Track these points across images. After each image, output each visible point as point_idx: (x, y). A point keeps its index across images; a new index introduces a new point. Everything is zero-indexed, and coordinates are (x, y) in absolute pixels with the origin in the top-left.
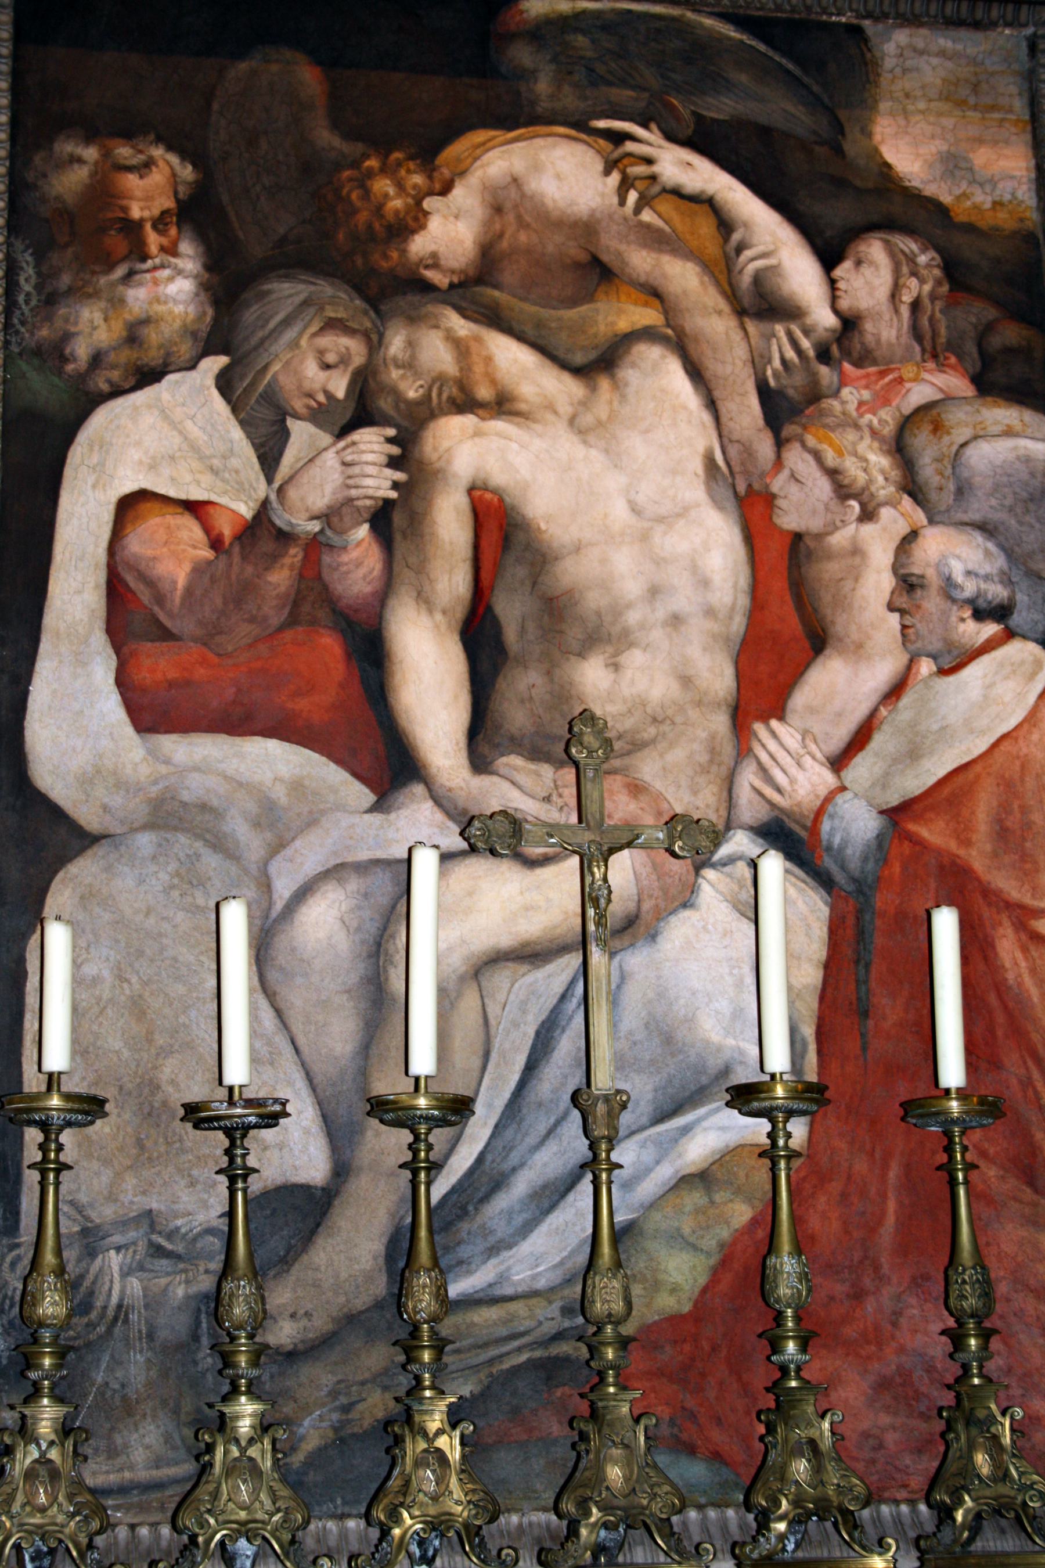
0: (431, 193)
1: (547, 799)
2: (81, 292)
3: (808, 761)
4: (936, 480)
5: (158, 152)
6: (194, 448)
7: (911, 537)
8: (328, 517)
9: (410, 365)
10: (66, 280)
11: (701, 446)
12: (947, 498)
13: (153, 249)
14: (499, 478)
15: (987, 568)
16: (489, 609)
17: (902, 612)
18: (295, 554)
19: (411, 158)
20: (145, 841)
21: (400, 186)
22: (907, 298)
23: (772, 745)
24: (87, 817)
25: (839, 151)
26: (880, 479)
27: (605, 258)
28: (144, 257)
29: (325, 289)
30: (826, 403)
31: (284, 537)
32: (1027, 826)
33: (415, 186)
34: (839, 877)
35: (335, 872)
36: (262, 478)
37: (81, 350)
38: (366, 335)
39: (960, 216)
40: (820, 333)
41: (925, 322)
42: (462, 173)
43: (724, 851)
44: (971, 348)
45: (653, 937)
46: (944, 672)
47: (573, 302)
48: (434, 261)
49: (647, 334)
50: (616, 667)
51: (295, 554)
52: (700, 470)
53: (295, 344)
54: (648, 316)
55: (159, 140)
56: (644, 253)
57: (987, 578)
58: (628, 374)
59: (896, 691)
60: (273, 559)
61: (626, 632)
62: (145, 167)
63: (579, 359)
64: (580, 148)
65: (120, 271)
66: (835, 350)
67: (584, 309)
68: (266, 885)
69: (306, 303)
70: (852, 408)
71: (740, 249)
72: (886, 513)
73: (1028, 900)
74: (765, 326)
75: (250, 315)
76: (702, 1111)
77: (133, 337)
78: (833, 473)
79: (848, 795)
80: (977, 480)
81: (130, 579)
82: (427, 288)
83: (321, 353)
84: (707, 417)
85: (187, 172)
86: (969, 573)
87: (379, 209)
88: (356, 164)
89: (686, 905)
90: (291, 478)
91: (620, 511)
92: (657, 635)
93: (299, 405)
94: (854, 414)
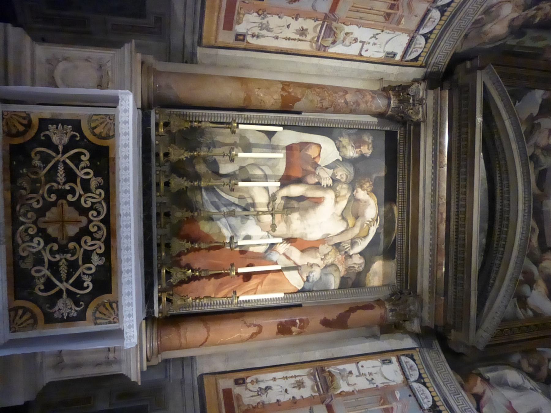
0: (367, 192)
2: (350, 138)
3: (284, 249)
4: (327, 270)
5: (371, 151)
7: (319, 266)
8: (319, 175)
9: (342, 188)
13: (357, 150)
15: (314, 278)
16: (306, 200)
17: (307, 265)
18: (313, 170)
19: (372, 189)
21: (367, 187)
22: (355, 266)
25: (377, 255)
26: (327, 261)
28: (355, 149)
29: (352, 175)
30: (339, 253)
31: (315, 169)
34: (266, 254)
37: (341, 139)
39: (368, 274)
40: (349, 252)
41: (351, 268)
42: (370, 197)
45: (257, 224)
48: (357, 192)
49: (348, 225)
50: (298, 219)
51: (313, 170)
53: (344, 171)
54: (350, 225)
55: (373, 151)
57: (313, 278)
58: (342, 221)
60: (312, 167)
62: (369, 149)
63: (343, 214)
64: (375, 215)
65: (353, 145)
66: (347, 254)
68: (263, 165)
69: (350, 172)
70: (338, 257)
71: (361, 239)
72: (322, 262)
73: (264, 284)
74: (350, 243)
75: (348, 165)
76: (231, 232)
78: (328, 254)
82: (353, 191)
83: (343, 175)
84: (336, 234)
85: (368, 155)
86: (314, 275)
87: (364, 184)
88: (371, 180)
89: (262, 229)
93: (335, 171)
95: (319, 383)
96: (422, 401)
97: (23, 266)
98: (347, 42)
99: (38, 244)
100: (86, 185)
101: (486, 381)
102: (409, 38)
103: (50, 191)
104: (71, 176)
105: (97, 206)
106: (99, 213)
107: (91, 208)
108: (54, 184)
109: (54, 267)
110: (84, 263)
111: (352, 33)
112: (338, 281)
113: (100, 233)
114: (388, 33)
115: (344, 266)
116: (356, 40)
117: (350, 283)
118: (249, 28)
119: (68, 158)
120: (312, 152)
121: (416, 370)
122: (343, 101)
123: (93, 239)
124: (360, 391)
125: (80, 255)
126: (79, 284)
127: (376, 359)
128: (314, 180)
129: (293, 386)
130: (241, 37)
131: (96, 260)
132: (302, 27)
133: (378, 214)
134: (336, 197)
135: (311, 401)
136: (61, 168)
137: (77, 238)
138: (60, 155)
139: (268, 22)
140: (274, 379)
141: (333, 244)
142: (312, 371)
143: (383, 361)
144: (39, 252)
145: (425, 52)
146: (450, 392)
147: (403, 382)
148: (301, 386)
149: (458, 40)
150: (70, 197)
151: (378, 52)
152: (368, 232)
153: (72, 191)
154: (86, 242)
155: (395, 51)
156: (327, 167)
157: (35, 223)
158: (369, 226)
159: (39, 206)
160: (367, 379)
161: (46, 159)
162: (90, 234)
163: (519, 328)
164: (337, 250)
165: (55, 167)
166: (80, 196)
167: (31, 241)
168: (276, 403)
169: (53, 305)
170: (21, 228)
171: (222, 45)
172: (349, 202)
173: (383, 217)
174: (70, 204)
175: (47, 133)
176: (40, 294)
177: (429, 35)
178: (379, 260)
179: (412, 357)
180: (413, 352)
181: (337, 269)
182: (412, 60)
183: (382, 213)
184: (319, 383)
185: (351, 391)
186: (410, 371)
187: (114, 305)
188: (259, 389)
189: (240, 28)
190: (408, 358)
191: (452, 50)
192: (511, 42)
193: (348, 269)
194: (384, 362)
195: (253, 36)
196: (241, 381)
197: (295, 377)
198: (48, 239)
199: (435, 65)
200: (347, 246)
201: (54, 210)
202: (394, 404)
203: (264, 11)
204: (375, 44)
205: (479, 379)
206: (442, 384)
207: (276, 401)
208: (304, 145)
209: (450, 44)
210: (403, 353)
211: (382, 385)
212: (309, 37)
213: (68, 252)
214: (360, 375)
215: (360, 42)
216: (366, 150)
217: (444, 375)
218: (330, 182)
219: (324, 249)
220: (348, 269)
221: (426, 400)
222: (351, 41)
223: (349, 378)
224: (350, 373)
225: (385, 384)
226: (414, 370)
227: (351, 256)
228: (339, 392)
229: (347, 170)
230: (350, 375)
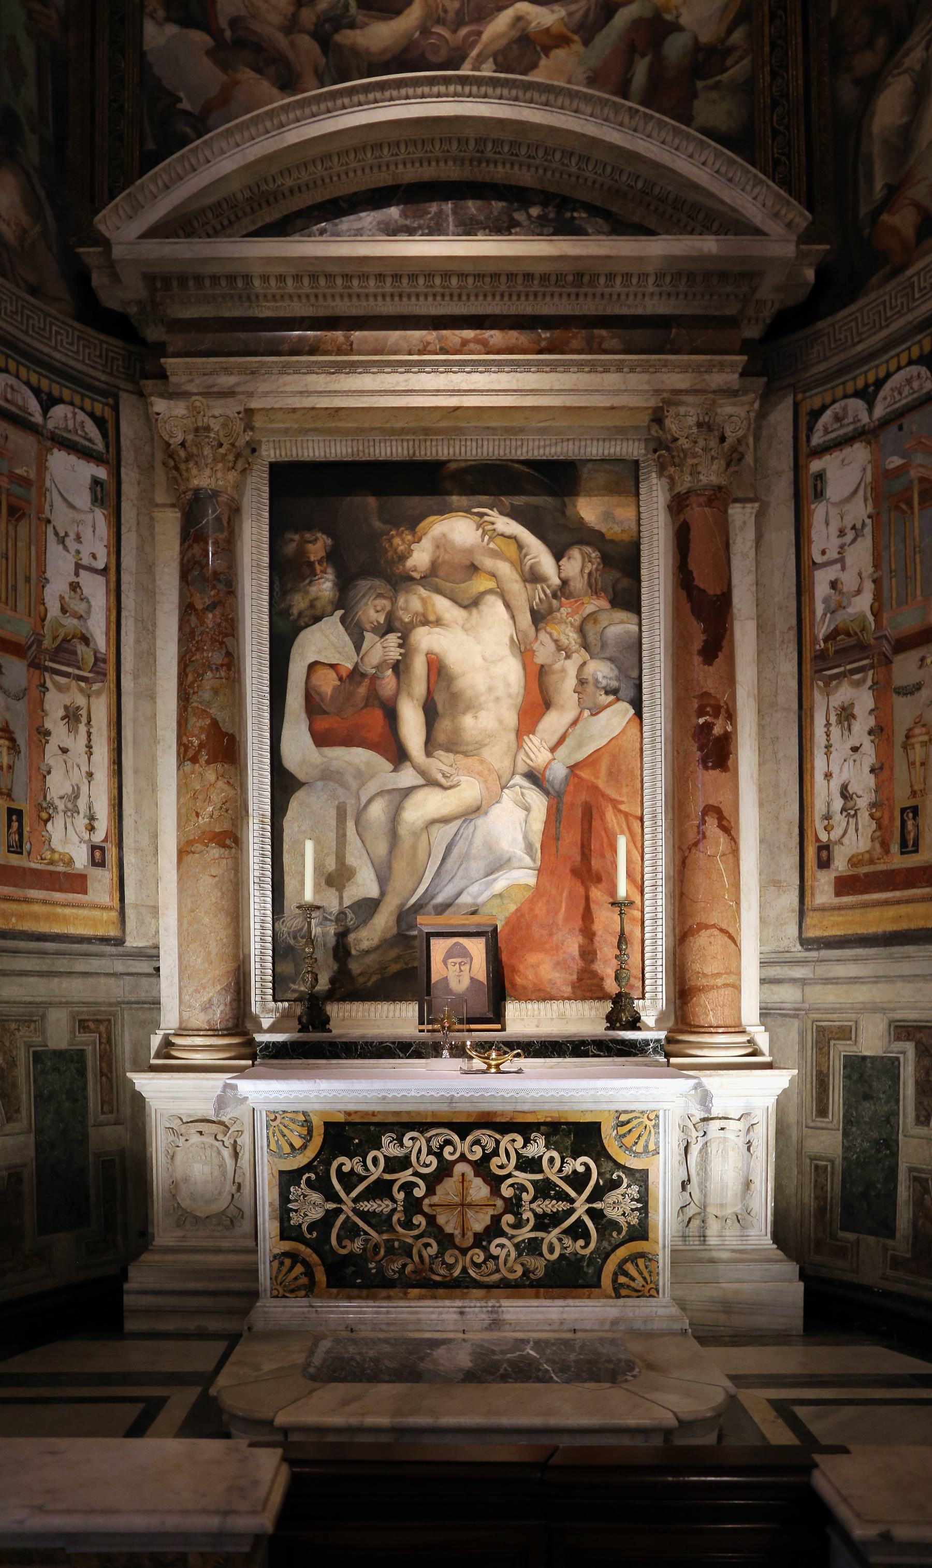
4: (594, 642)
5: (319, 535)
6: (333, 645)
7: (584, 663)
8: (377, 667)
9: (406, 609)
10: (289, 586)
12: (598, 649)
14: (436, 648)
15: (611, 675)
18: (367, 682)
21: (403, 540)
22: (587, 571)
23: (530, 744)
24: (301, 776)
29: (377, 582)
31: (363, 675)
32: (619, 771)
34: (552, 791)
35: (380, 794)
37: (295, 611)
38: (391, 598)
40: (554, 587)
44: (611, 590)
45: (486, 813)
46: (592, 715)
48: (415, 569)
49: (491, 591)
53: (366, 604)
54: (491, 584)
57: (611, 679)
58: (483, 607)
59: (575, 723)
60: (360, 683)
61: (480, 705)
63: (466, 603)
65: (307, 581)
67: (468, 583)
69: (370, 588)
71: (525, 556)
72: (575, 655)
75: (351, 594)
77: (312, 606)
78: (556, 641)
80: (609, 641)
81: (314, 695)
82: (412, 579)
84: (511, 622)
85: (329, 542)
87: (395, 551)
88: (388, 534)
91: (479, 661)
92: (491, 705)
93: (368, 626)
95: (849, 667)
96: (915, 396)
97: (540, 1273)
98: (81, 608)
99: (501, 1248)
100: (397, 1164)
101: (893, 191)
102: (55, 451)
103: (408, 1224)
104: (381, 1189)
105: (435, 1144)
106: (448, 1142)
107: (439, 1155)
108: (395, 1218)
109: (544, 1222)
110: (541, 1171)
111: (62, 598)
112: (621, 615)
113: (485, 1140)
114: (52, 506)
115: (586, 600)
116: (75, 587)
117: (625, 583)
118: (77, 840)
119: (348, 1194)
120: (327, 683)
121: (846, 405)
122: (210, 616)
123: (495, 1153)
124: (876, 566)
125: (522, 1177)
126: (578, 1181)
127: (810, 513)
128: (388, 680)
129: (846, 733)
130: (98, 854)
131: (537, 1148)
132: (63, 718)
134: (426, 622)
135: (882, 690)
136: (366, 1206)
137: (495, 1182)
138: (344, 1207)
139: (62, 798)
140: (828, 776)
141: (533, 628)
142: (821, 683)
143: (816, 497)
144: (517, 1246)
145: (82, 400)
146: (905, 309)
147: (869, 443)
148: (849, 712)
149: (46, 314)
150: (419, 1193)
151: (94, 527)
152: (509, 537)
153: (408, 1187)
154: (502, 1167)
155: (88, 481)
156: (358, 647)
157: (464, 1252)
159: (435, 1244)
160: (854, 541)
161: (351, 1231)
162: (486, 1158)
163: (774, 75)
165: (363, 1215)
166: (416, 1174)
167: (496, 1258)
168: (876, 776)
169: (615, 1225)
170: (473, 1274)
171: (117, 896)
172: (439, 591)
173: (471, 497)
174: (431, 1191)
175: (304, 1227)
176: (592, 1245)
177: (45, 398)
178: (575, 506)
179: (816, 414)
180: (805, 407)
181: (592, 617)
182: (104, 435)
183: (464, 500)
184: (849, 667)
185: (873, 586)
186: (846, 422)
187: (623, 1118)
188: (845, 814)
189: (81, 858)
190: (816, 427)
191: (71, 326)
192: (32, 154)
193: (594, 589)
194: (819, 494)
195: (91, 829)
196: (824, 853)
197: (828, 725)
198: (494, 1230)
199: (108, 370)
201: (441, 1220)
202: (914, 474)
203: (41, 808)
204: (78, 538)
205: (885, 217)
206: (884, 333)
207: (872, 776)
209: (57, 333)
210: (804, 438)
211: (870, 501)
212: (81, 701)
213: (520, 1199)
214: (841, 560)
215: (77, 574)
217: (864, 325)
218: (393, 639)
219: (544, 652)
221: (916, 385)
222: (78, 597)
223: (845, 590)
224: (834, 585)
225: (869, 495)
226: (845, 409)
227: (565, 582)
228: (871, 618)
229: (364, 596)
230: (839, 586)
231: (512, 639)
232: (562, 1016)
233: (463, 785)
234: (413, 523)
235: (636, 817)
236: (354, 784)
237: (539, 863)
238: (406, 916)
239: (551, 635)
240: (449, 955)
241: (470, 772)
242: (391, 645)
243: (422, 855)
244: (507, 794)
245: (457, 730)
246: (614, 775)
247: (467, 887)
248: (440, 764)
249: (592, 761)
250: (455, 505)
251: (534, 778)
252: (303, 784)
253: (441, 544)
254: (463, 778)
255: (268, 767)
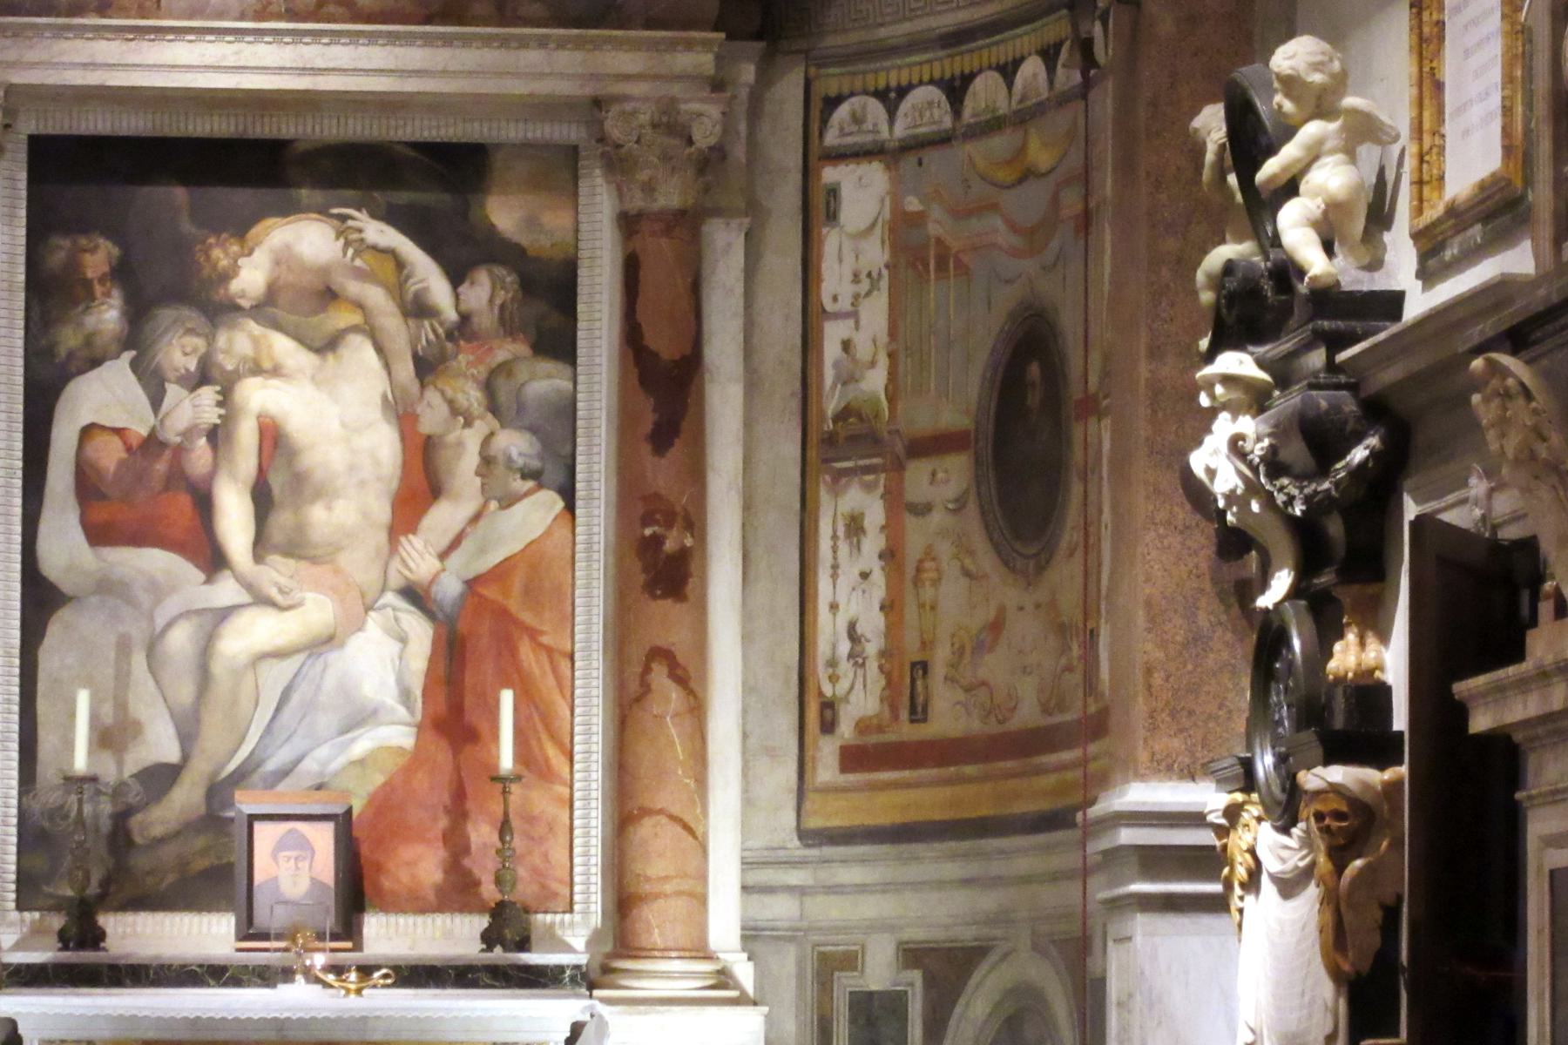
0: (243, 255)
1: (291, 577)
3: (427, 555)
5: (101, 241)
7: (492, 434)
8: (189, 433)
11: (380, 390)
18: (167, 454)
19: (232, 235)
20: (94, 600)
21: (227, 254)
22: (498, 302)
23: (408, 547)
26: (476, 405)
27: (334, 287)
28: (94, 299)
31: (163, 445)
33: (234, 253)
34: (440, 616)
36: (152, 415)
37: (62, 351)
39: (531, 253)
43: (381, 602)
45: (342, 645)
47: (316, 312)
52: (379, 402)
53: (170, 343)
54: (355, 318)
56: (355, 283)
59: (476, 518)
60: (158, 456)
62: (93, 250)
63: (317, 344)
65: (80, 308)
66: (456, 333)
67: (322, 316)
70: (463, 365)
71: (408, 277)
72: (478, 423)
76: (362, 730)
78: (451, 403)
79: (447, 573)
82: (237, 308)
83: (183, 347)
84: (384, 374)
85: (116, 251)
86: (520, 454)
87: (215, 267)
88: (204, 242)
90: (167, 414)
91: (335, 426)
93: (171, 375)
94: (464, 369)
112: (547, 366)
117: (555, 319)
133: (320, 213)
134: (257, 370)
156: (156, 401)
158: (363, 248)
164: (441, 367)
172: (277, 326)
178: (482, 206)
181: (505, 369)
193: (508, 325)
200: (427, 329)
208: (87, 486)
216: (99, 257)
218: (208, 394)
219: (432, 415)
220: (508, 325)
227: (465, 318)
229: (166, 331)
231: (385, 398)
232: (448, 935)
233: (309, 604)
234: (240, 228)
235: (563, 654)
236: (145, 599)
237: (419, 717)
238: (219, 791)
239: (443, 393)
240: (281, 846)
241: (317, 587)
242: (203, 406)
243: (245, 702)
244: (374, 621)
245: (301, 529)
246: (531, 593)
247: (311, 750)
248: (275, 573)
249: (500, 573)
250: (305, 201)
251: (415, 595)
252: (70, 599)
253: (283, 259)
254: (310, 596)
255: (17, 576)
